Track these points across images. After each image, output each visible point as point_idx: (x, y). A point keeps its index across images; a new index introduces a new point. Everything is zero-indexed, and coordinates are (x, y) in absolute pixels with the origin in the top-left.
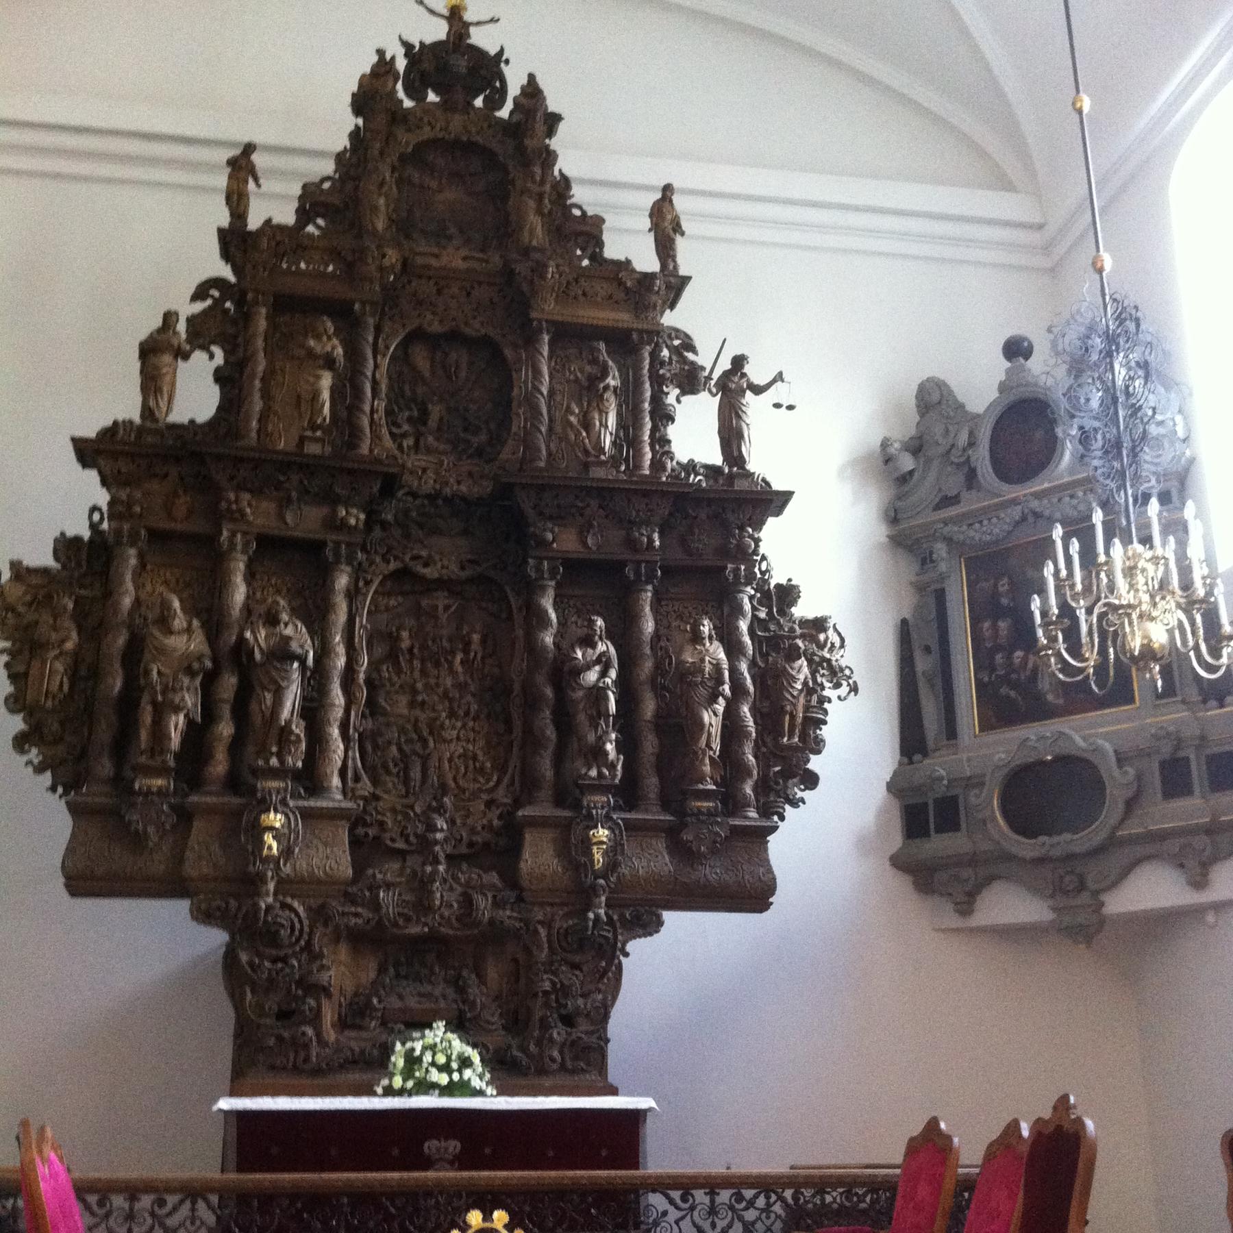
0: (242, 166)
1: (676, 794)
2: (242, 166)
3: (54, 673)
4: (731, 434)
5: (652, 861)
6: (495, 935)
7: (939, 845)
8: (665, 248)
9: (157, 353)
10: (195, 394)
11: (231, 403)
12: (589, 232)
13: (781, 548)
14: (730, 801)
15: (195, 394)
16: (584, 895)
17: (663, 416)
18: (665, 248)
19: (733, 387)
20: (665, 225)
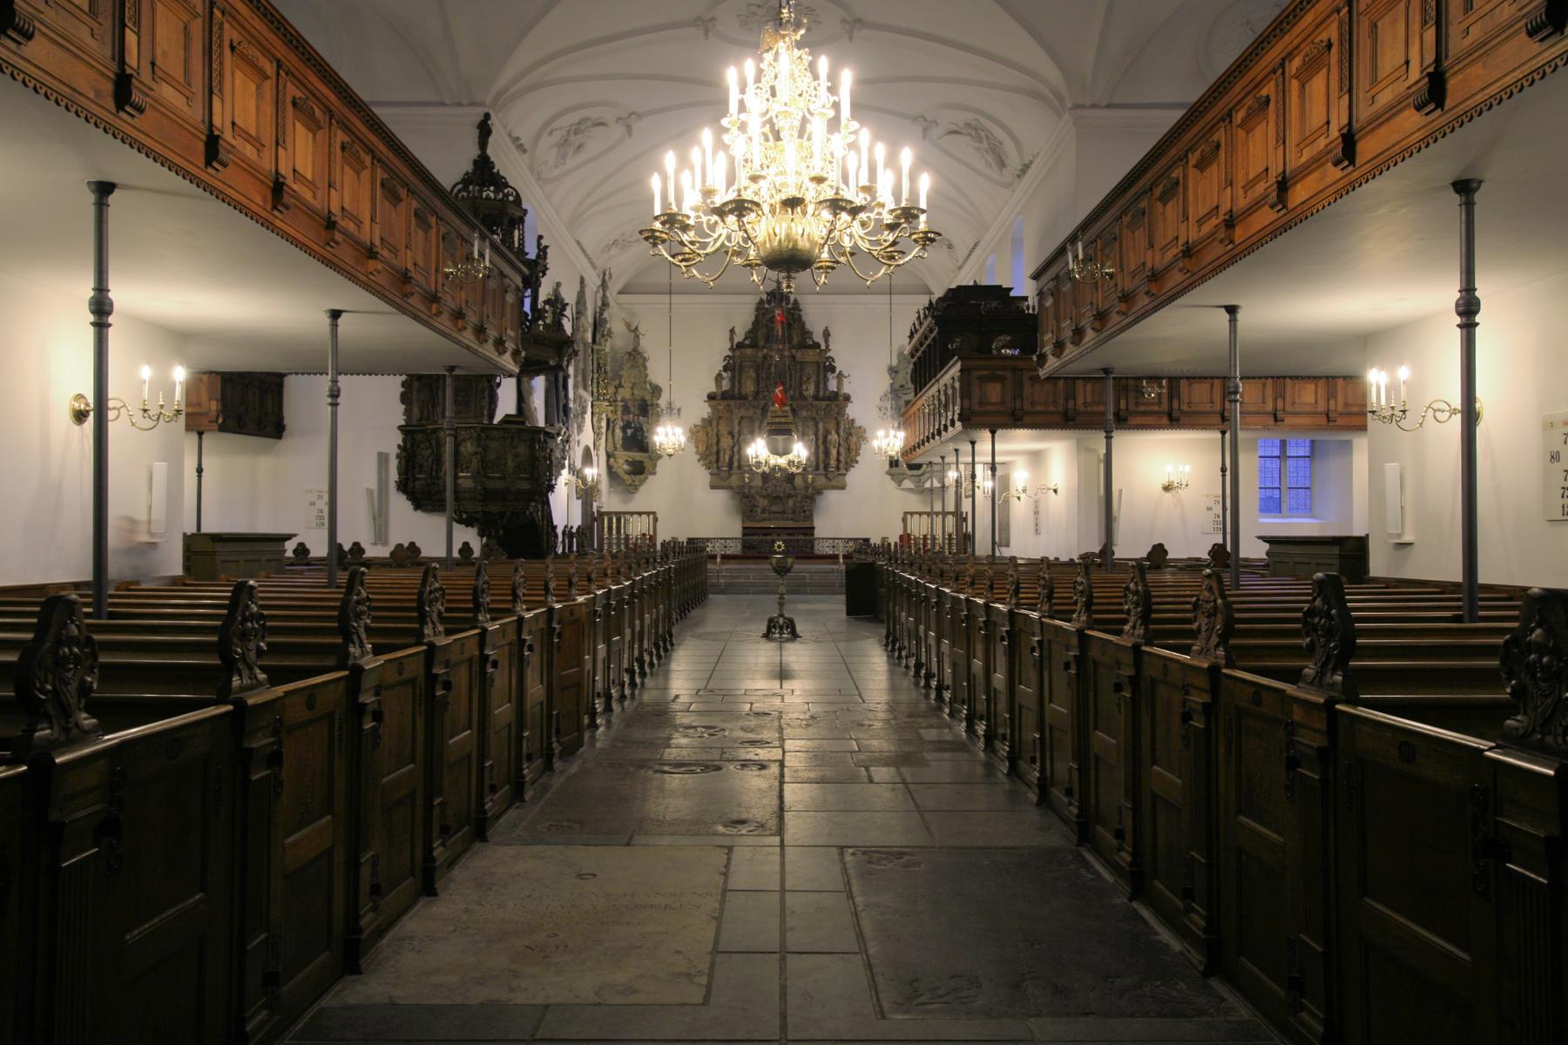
0: (732, 331)
1: (826, 467)
2: (732, 331)
3: (702, 448)
4: (840, 385)
5: (821, 481)
6: (789, 496)
7: (895, 470)
8: (827, 342)
9: (719, 378)
10: (726, 385)
11: (733, 385)
12: (808, 334)
13: (852, 411)
14: (838, 468)
15: (726, 385)
16: (807, 488)
17: (826, 380)
18: (827, 342)
19: (840, 376)
20: (827, 334)
